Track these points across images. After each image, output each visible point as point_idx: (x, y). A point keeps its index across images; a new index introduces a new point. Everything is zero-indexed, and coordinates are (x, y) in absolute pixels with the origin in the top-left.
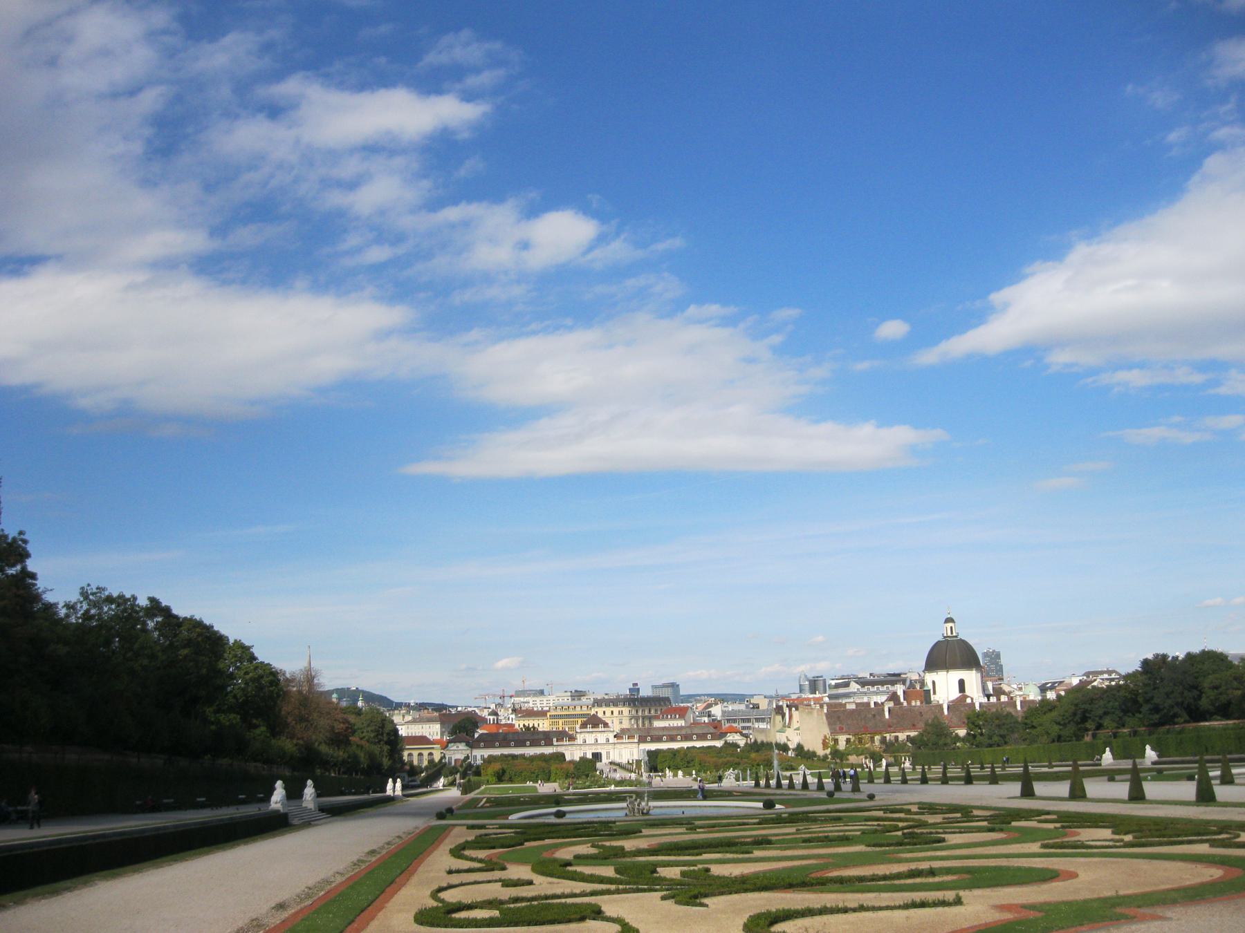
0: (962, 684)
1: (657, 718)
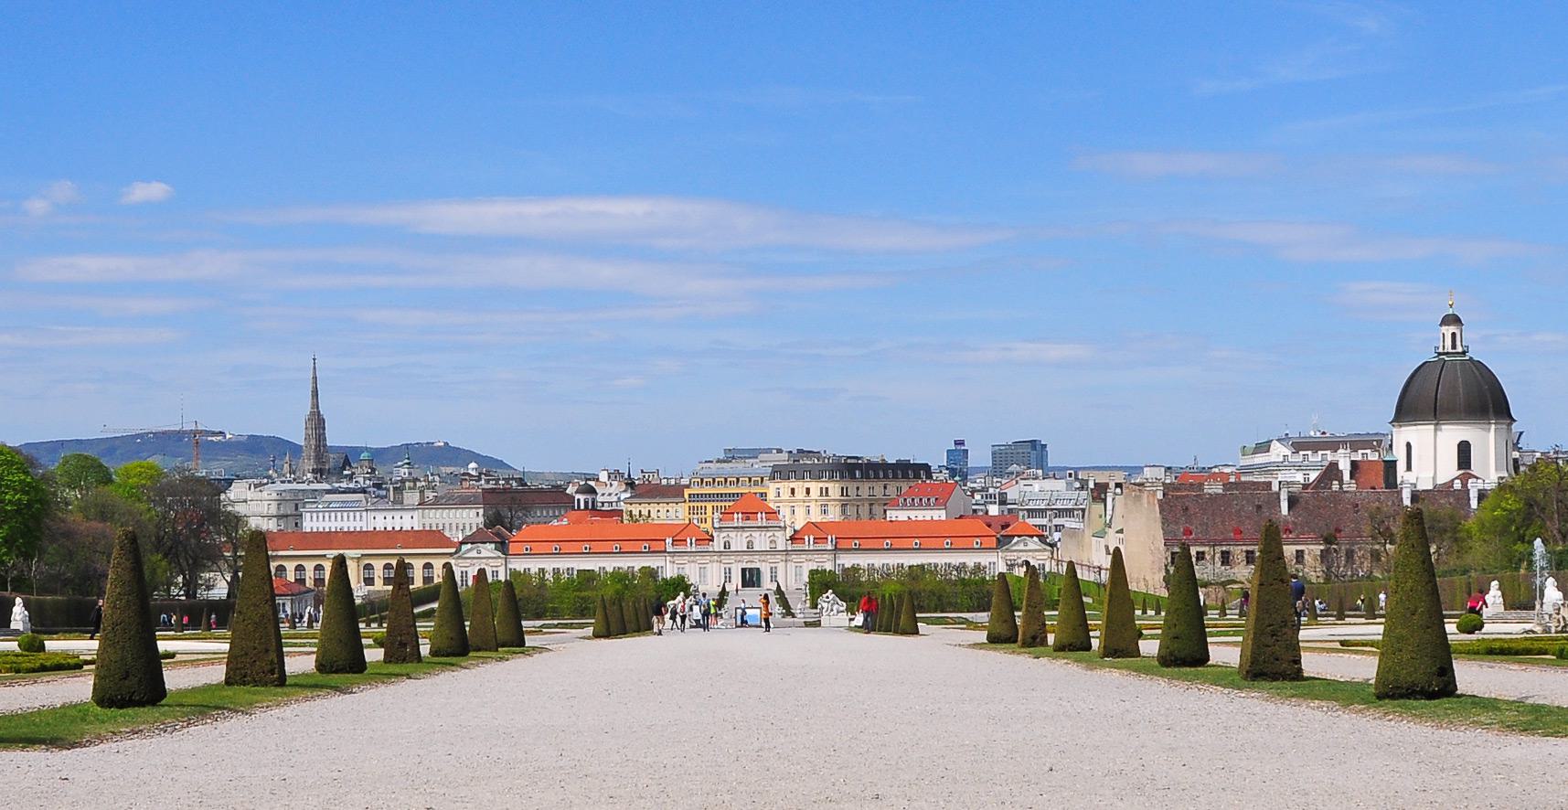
0: (1464, 450)
1: (894, 504)
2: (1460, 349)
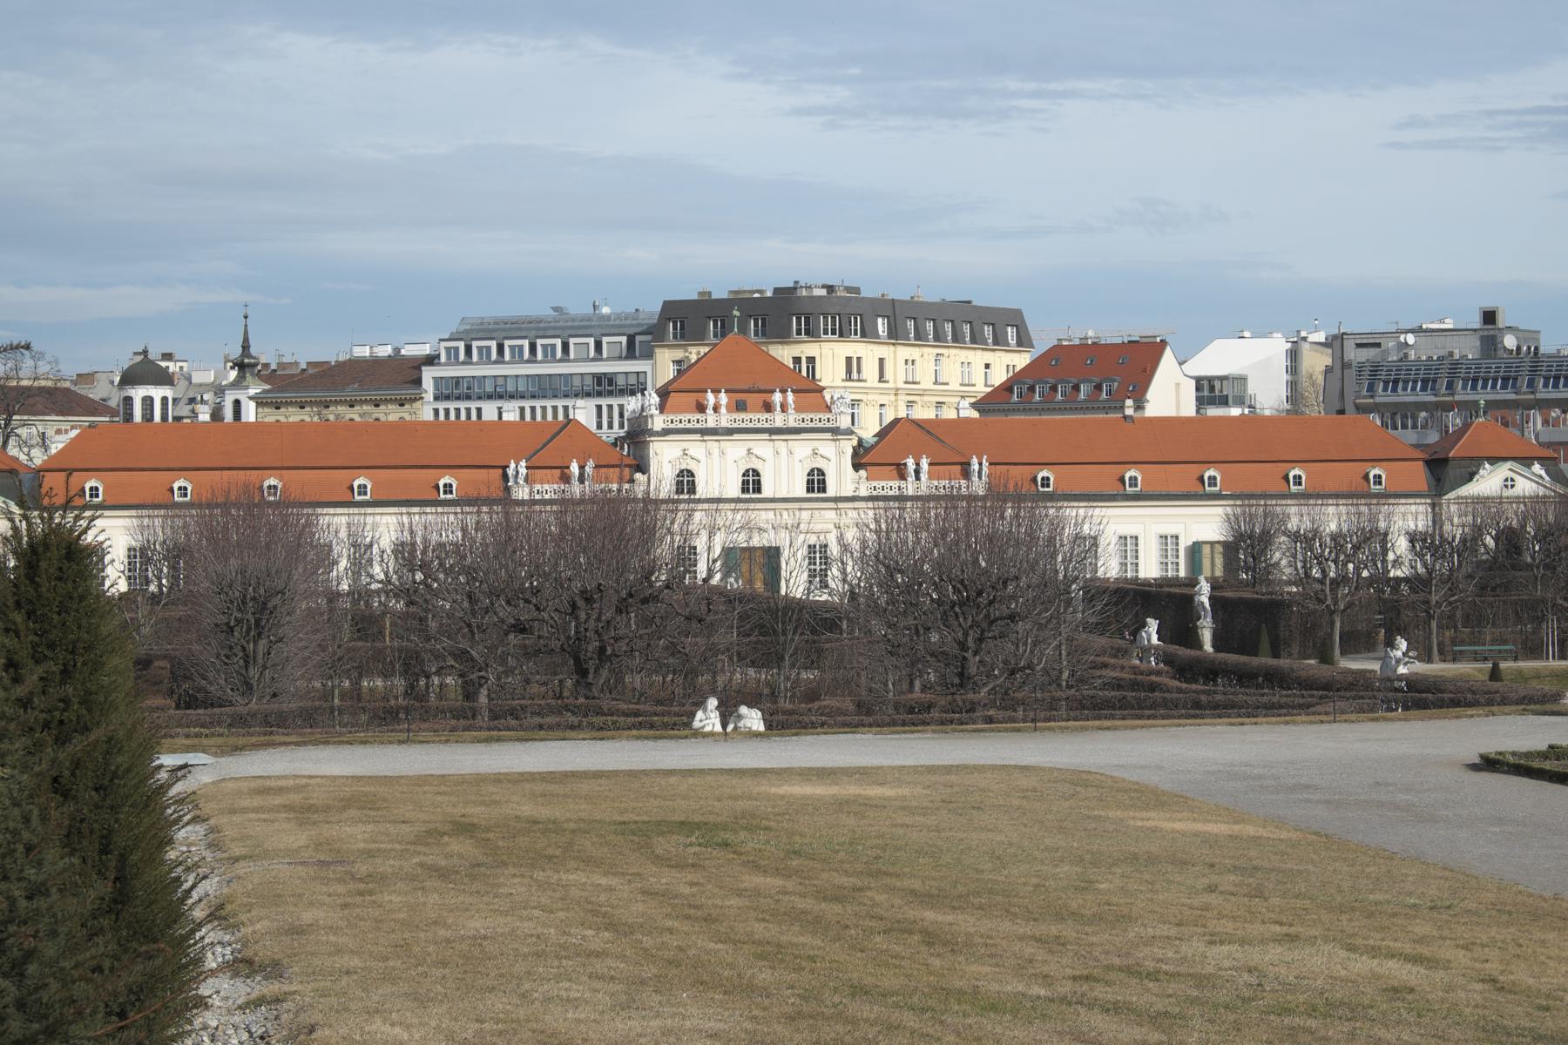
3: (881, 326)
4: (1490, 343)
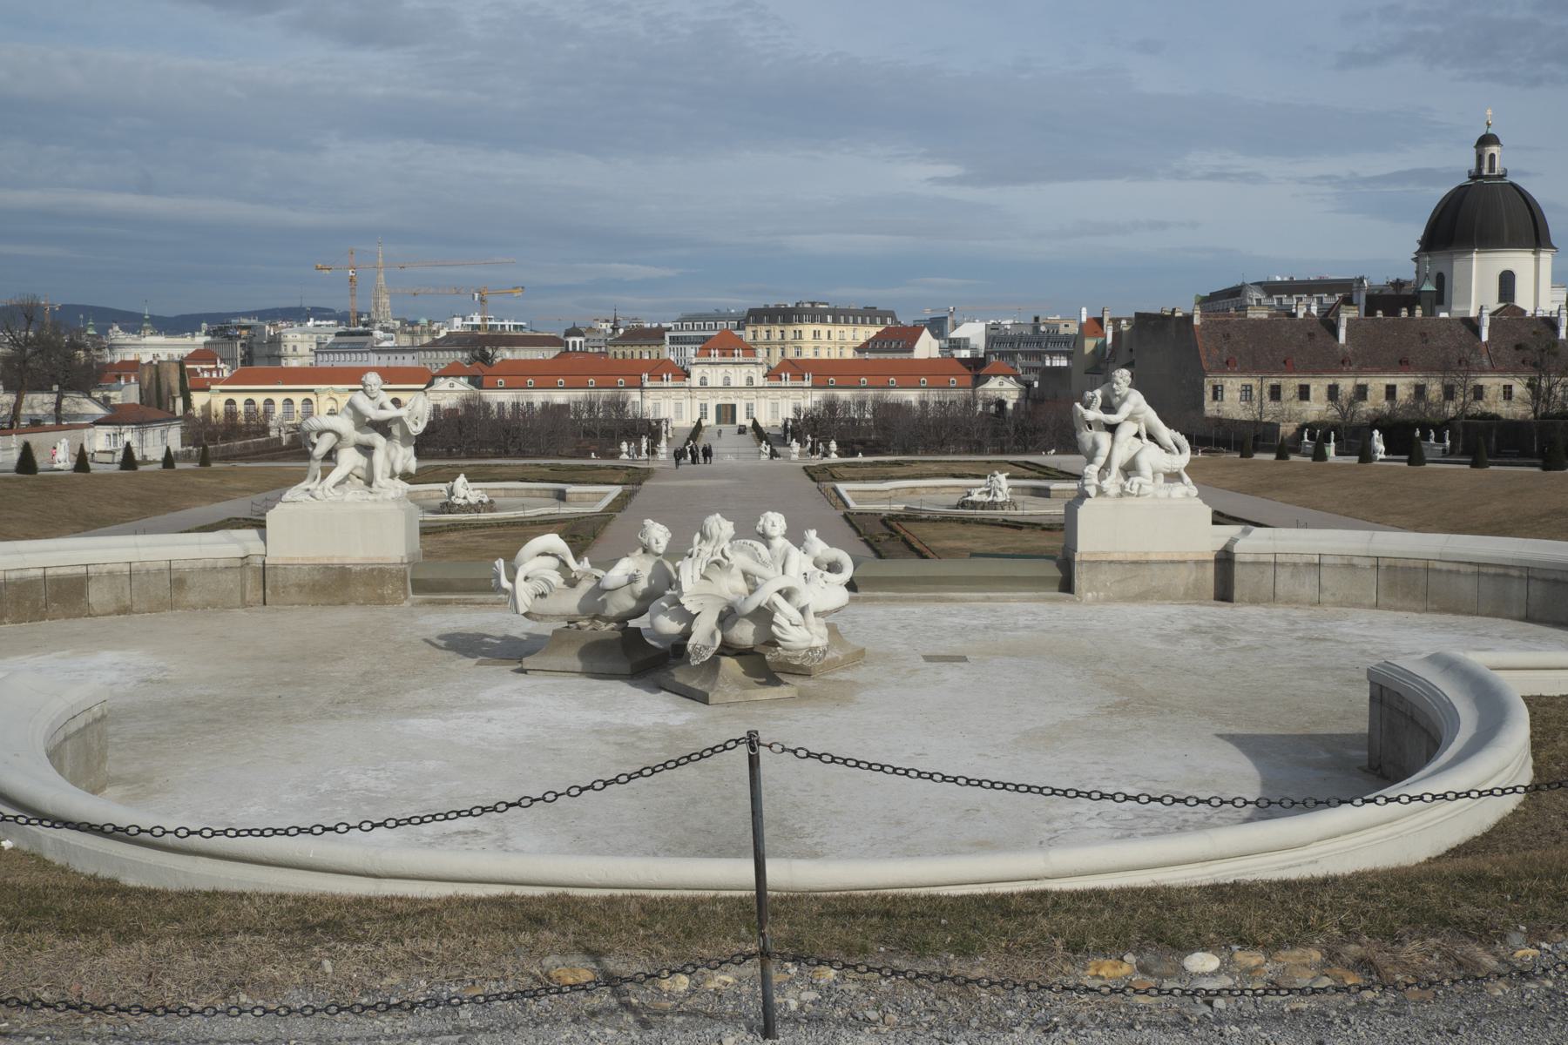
2: (1498, 169)
3: (829, 318)
4: (1036, 328)
